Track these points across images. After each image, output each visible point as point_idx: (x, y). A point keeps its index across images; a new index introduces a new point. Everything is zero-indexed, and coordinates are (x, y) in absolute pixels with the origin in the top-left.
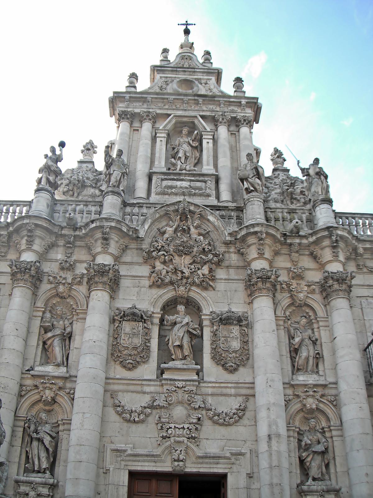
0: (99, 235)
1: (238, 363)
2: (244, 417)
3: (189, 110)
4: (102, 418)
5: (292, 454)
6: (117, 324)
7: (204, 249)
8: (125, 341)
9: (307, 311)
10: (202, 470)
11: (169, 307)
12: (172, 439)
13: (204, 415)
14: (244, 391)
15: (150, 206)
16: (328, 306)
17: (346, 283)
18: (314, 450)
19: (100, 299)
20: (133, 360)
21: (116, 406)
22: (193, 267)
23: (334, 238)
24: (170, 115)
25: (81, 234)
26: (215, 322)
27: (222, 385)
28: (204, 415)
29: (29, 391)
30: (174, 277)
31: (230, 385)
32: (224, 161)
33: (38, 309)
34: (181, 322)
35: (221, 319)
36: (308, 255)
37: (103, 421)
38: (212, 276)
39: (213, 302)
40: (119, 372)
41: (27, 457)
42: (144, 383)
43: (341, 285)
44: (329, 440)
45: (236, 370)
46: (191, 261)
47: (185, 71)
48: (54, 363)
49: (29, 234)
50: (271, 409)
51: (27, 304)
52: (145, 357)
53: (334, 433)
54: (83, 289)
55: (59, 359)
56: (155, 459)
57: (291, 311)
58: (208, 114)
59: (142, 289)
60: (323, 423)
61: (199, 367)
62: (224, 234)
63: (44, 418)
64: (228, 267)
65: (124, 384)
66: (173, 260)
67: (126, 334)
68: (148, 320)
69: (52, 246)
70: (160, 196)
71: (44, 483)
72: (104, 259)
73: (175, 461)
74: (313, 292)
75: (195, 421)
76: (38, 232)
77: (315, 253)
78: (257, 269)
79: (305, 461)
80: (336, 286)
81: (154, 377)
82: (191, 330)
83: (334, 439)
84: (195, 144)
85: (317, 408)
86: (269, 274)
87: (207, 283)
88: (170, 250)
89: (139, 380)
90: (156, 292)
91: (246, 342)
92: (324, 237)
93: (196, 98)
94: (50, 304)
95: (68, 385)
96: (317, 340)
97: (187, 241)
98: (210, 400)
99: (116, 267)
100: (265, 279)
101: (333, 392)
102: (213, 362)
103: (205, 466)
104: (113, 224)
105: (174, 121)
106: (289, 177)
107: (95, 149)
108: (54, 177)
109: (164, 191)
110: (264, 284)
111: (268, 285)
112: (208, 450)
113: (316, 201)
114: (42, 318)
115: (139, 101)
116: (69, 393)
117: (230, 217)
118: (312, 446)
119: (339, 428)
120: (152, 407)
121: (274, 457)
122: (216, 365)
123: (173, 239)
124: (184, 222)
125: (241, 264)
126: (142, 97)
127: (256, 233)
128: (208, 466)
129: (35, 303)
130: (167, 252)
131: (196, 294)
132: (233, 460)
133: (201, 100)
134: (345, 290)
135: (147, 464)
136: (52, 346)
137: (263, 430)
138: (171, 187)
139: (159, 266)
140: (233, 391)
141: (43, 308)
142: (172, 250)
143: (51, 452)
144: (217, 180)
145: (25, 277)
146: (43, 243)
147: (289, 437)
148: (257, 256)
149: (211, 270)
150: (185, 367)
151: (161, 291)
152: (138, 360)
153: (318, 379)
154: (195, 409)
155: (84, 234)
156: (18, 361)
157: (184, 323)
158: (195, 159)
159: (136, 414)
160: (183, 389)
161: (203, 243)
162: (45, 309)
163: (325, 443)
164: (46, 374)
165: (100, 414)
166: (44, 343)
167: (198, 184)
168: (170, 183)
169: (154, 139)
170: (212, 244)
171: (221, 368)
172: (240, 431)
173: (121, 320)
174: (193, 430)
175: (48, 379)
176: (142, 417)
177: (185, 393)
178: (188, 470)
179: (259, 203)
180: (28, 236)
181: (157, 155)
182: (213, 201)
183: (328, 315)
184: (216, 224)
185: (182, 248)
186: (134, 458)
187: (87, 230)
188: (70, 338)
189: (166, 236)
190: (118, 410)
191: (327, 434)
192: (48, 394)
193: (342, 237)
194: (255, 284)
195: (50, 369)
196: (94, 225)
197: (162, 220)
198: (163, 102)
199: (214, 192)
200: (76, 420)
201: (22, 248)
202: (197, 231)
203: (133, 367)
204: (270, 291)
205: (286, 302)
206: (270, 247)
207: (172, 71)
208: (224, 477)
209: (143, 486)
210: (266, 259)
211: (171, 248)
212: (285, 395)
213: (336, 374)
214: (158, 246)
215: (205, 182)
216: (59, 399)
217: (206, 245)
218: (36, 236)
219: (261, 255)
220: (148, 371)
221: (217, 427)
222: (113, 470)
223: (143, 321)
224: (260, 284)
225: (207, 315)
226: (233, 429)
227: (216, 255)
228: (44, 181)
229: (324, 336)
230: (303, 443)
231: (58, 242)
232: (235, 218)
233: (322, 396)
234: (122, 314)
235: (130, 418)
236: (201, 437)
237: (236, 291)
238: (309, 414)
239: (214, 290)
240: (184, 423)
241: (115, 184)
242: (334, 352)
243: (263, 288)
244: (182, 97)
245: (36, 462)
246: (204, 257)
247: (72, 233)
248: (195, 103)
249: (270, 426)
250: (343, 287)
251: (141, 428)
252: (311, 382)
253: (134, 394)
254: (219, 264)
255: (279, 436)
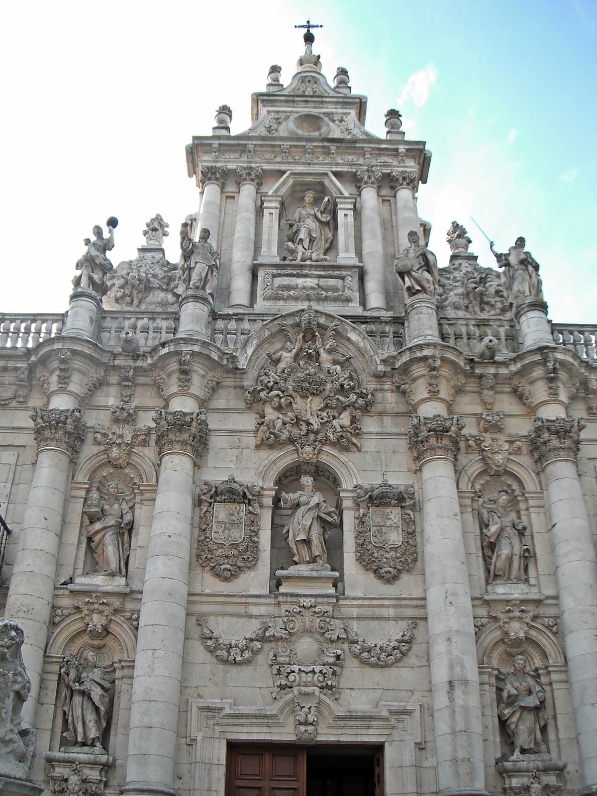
0: (174, 366)
1: (400, 568)
2: (410, 653)
3: (314, 164)
4: (183, 658)
5: (488, 712)
6: (206, 508)
7: (342, 386)
8: (218, 534)
9: (509, 482)
10: (343, 739)
11: (288, 478)
12: (296, 690)
13: (346, 650)
14: (409, 612)
15: (255, 317)
16: (542, 475)
17: (571, 437)
18: (522, 704)
19: (177, 467)
20: (231, 565)
21: (205, 638)
22: (324, 414)
23: (550, 365)
24: (284, 172)
25: (145, 364)
26: (361, 501)
27: (375, 602)
28: (346, 650)
29: (67, 616)
30: (295, 431)
31: (386, 602)
32: (373, 245)
33: (79, 486)
34: (308, 503)
35: (370, 497)
36: (509, 393)
37: (185, 661)
38: (357, 428)
39: (359, 471)
40: (210, 584)
41: (65, 721)
42: (250, 600)
43: (562, 441)
44: (547, 688)
45: (396, 578)
46: (322, 405)
47: (307, 102)
48: (106, 571)
49: (62, 366)
50: (454, 640)
51: (62, 477)
52: (251, 559)
53: (554, 677)
54: (150, 452)
55: (114, 565)
56: (269, 721)
57: (482, 482)
58: (345, 169)
59: (245, 451)
60: (536, 661)
61: (337, 574)
62: (374, 361)
63: (91, 658)
64: (380, 414)
65: (218, 602)
66: (294, 405)
67: (219, 523)
68: (255, 500)
69: (99, 385)
70: (271, 302)
71: (92, 761)
72: (183, 405)
73: (301, 724)
74: (518, 452)
75: (331, 660)
76: (77, 363)
77: (520, 389)
78: (427, 416)
79: (508, 722)
80: (555, 442)
81: (266, 591)
82: (323, 516)
83: (555, 686)
84: (326, 218)
85: (526, 638)
86: (448, 424)
87: (348, 440)
88: (288, 388)
89: (242, 596)
90: (266, 456)
91: (411, 533)
92: (534, 364)
93: (326, 144)
94: (98, 478)
95: (129, 606)
96: (525, 528)
97: (315, 374)
98: (355, 626)
99: (203, 417)
100: (440, 431)
101: (552, 611)
102: (360, 566)
103: (348, 731)
104: (196, 348)
105: (291, 182)
106: (477, 269)
107: (166, 229)
108: (101, 274)
109: (277, 294)
110: (440, 441)
111: (446, 442)
112: (353, 707)
113: (521, 305)
114: (86, 500)
115: (235, 151)
116: (130, 618)
117: (383, 335)
118: (520, 698)
119: (563, 669)
120: (262, 639)
121: (459, 717)
122: (365, 571)
123: (293, 370)
124: (310, 342)
125: (402, 408)
126: (239, 145)
127: (425, 359)
128: (354, 732)
129: (73, 478)
130: (283, 392)
131: (330, 457)
132: (393, 722)
133: (333, 147)
134: (569, 448)
135: (255, 729)
136: (101, 545)
137: (441, 674)
138: (288, 288)
139: (271, 414)
140: (392, 612)
141: (86, 483)
142: (290, 388)
143: (102, 713)
144: (362, 275)
145: (57, 436)
146: (86, 380)
147: (482, 684)
148: (428, 396)
149: (354, 420)
150: (315, 574)
151: (275, 455)
152: (239, 564)
153: (527, 591)
154: (332, 641)
155: (149, 365)
156: (48, 569)
157: (312, 504)
158: (326, 242)
159: (238, 651)
160: (313, 610)
161: (341, 376)
162: (90, 485)
163: (541, 694)
164: (93, 588)
165: (180, 651)
166: (90, 540)
167: (332, 282)
168: (286, 281)
169: (259, 211)
170: (355, 377)
171: (372, 575)
172: (405, 675)
173: (212, 500)
174: (329, 675)
175: (96, 597)
176: (247, 655)
177: (315, 616)
178: (321, 738)
179: (430, 311)
180: (61, 370)
181: (265, 237)
182: (355, 308)
183: (543, 488)
184: (361, 345)
185: (308, 385)
186: (236, 721)
187: (156, 358)
188: (130, 531)
189: (282, 365)
190: (208, 644)
191: (544, 679)
192: (97, 621)
193: (563, 363)
194: (424, 440)
195: (99, 581)
196: (165, 350)
197: (274, 341)
198: (273, 152)
199: (357, 294)
200: (142, 661)
201: (51, 390)
202: (330, 358)
203: (232, 575)
204: (450, 451)
205: (475, 468)
206: (448, 381)
207: (286, 101)
209: (249, 765)
210: (443, 400)
211: (290, 386)
212: (475, 618)
213: (556, 583)
214: (269, 382)
215: (343, 278)
216: (114, 628)
217: (345, 380)
218: (74, 369)
219: (434, 394)
220: (256, 580)
221: (368, 670)
222: (203, 739)
223: (247, 501)
224: (433, 441)
225: (348, 491)
226: (393, 672)
227: (361, 395)
228: (84, 282)
229: (536, 521)
230: (505, 694)
231: (108, 377)
232: (391, 336)
233: (535, 618)
234: (212, 492)
235: (227, 657)
236: (341, 686)
237: (394, 452)
238: (514, 647)
239: (360, 451)
240: (314, 664)
241: (198, 284)
242: (552, 548)
243: (439, 447)
244: (304, 144)
245: (80, 729)
246: (342, 398)
247: (131, 363)
248: (324, 153)
249: (451, 667)
250: (566, 444)
251: (245, 672)
252: (516, 596)
253: (235, 619)
254: (366, 409)
255: (465, 682)
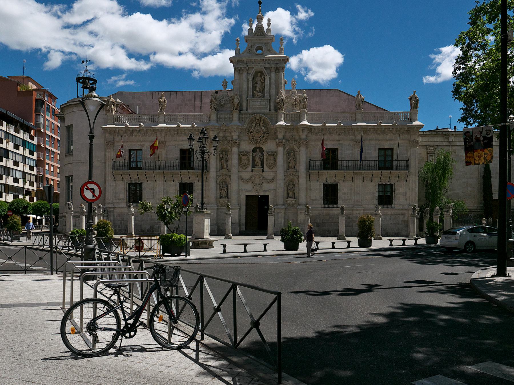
11: (254, 151)
144: (270, 100)
220: (250, 169)
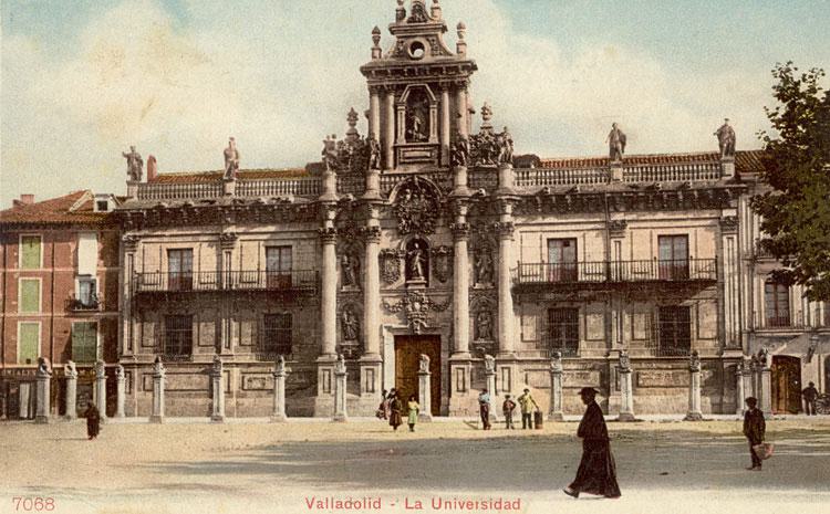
11: (410, 246)
208: (439, 337)
